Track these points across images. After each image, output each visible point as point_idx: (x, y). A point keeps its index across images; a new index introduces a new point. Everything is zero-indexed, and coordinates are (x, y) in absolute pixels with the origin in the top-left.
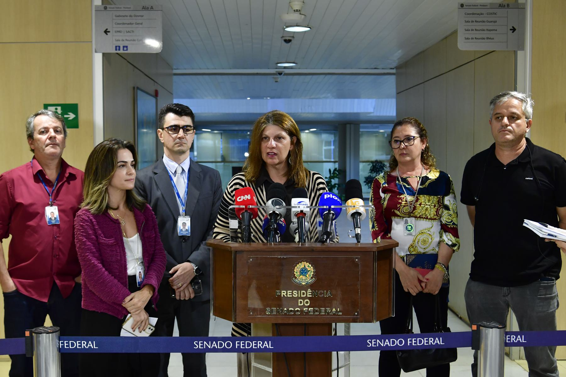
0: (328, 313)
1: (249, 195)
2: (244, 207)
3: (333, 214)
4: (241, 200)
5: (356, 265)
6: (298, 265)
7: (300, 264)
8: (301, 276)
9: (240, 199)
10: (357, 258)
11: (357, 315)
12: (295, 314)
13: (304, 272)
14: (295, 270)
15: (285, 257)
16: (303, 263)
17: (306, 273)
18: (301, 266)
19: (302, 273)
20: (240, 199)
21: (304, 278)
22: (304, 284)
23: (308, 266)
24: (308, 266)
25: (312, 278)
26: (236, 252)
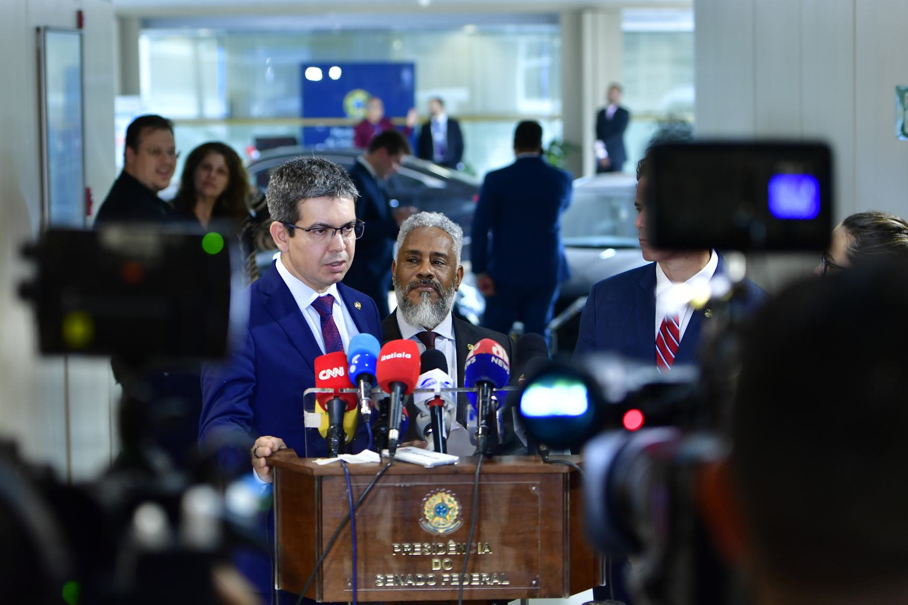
0: (485, 582)
1: (342, 368)
2: (331, 391)
3: (496, 401)
5: (534, 498)
6: (431, 500)
7: (434, 497)
8: (437, 519)
9: (325, 375)
10: (534, 485)
11: (535, 585)
12: (426, 586)
13: (441, 510)
14: (426, 509)
15: (408, 485)
16: (439, 494)
17: (444, 512)
18: (435, 500)
19: (439, 513)
20: (325, 375)
21: (441, 521)
22: (441, 531)
23: (450, 501)
24: (450, 501)
25: (456, 520)
26: (321, 478)
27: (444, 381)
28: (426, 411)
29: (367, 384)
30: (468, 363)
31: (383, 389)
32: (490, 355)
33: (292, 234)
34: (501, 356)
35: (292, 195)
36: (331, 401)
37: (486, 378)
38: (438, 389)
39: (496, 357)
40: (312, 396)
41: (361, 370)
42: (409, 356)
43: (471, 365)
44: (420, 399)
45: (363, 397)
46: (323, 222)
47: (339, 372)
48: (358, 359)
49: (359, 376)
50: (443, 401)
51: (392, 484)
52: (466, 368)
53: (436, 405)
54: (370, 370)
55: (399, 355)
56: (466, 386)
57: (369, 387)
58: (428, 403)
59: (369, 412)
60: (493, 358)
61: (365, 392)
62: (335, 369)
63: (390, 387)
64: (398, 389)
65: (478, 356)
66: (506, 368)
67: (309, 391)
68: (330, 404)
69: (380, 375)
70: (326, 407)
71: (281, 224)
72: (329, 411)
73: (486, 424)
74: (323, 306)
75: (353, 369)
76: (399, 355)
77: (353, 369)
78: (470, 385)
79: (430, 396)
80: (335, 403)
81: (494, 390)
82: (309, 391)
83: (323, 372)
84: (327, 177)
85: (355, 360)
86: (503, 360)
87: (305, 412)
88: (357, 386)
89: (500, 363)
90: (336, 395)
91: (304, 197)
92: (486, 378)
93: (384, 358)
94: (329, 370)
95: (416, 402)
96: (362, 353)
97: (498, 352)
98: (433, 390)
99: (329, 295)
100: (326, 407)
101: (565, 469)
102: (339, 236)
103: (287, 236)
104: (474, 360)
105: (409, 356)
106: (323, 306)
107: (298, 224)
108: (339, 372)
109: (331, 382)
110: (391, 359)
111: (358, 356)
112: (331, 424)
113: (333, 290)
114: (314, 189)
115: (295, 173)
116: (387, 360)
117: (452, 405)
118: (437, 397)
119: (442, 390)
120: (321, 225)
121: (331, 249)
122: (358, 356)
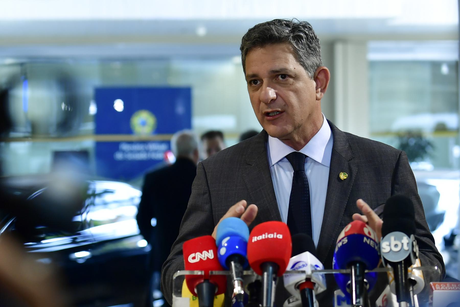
1: (211, 252)
4: (197, 260)
9: (194, 258)
20: (194, 258)
27: (314, 264)
28: (297, 294)
29: (238, 266)
30: (340, 244)
31: (255, 270)
32: (362, 235)
34: (372, 237)
36: (201, 284)
37: (358, 258)
38: (309, 271)
39: (368, 238)
40: (181, 278)
41: (231, 252)
43: (343, 246)
44: (291, 281)
45: (235, 278)
47: (209, 254)
48: (228, 242)
49: (230, 258)
50: (314, 284)
52: (337, 250)
53: (307, 286)
54: (242, 252)
55: (271, 236)
56: (335, 268)
58: (299, 286)
59: (242, 292)
60: (365, 239)
61: (236, 273)
62: (205, 252)
63: (261, 268)
64: (271, 268)
65: (349, 237)
67: (179, 273)
68: (200, 288)
69: (251, 257)
70: (196, 291)
72: (198, 295)
75: (223, 251)
76: (271, 236)
77: (223, 251)
78: (340, 265)
79: (301, 278)
80: (205, 286)
81: (366, 271)
82: (179, 273)
83: (193, 255)
85: (225, 243)
86: (374, 241)
87: (174, 296)
88: (229, 268)
90: (206, 278)
92: (358, 258)
93: (255, 239)
95: (286, 285)
96: (232, 235)
97: (369, 233)
98: (304, 272)
100: (196, 291)
104: (346, 241)
105: (280, 236)
108: (210, 254)
109: (201, 264)
110: (262, 240)
111: (228, 238)
117: (321, 287)
118: (308, 279)
119: (313, 272)
122: (228, 238)
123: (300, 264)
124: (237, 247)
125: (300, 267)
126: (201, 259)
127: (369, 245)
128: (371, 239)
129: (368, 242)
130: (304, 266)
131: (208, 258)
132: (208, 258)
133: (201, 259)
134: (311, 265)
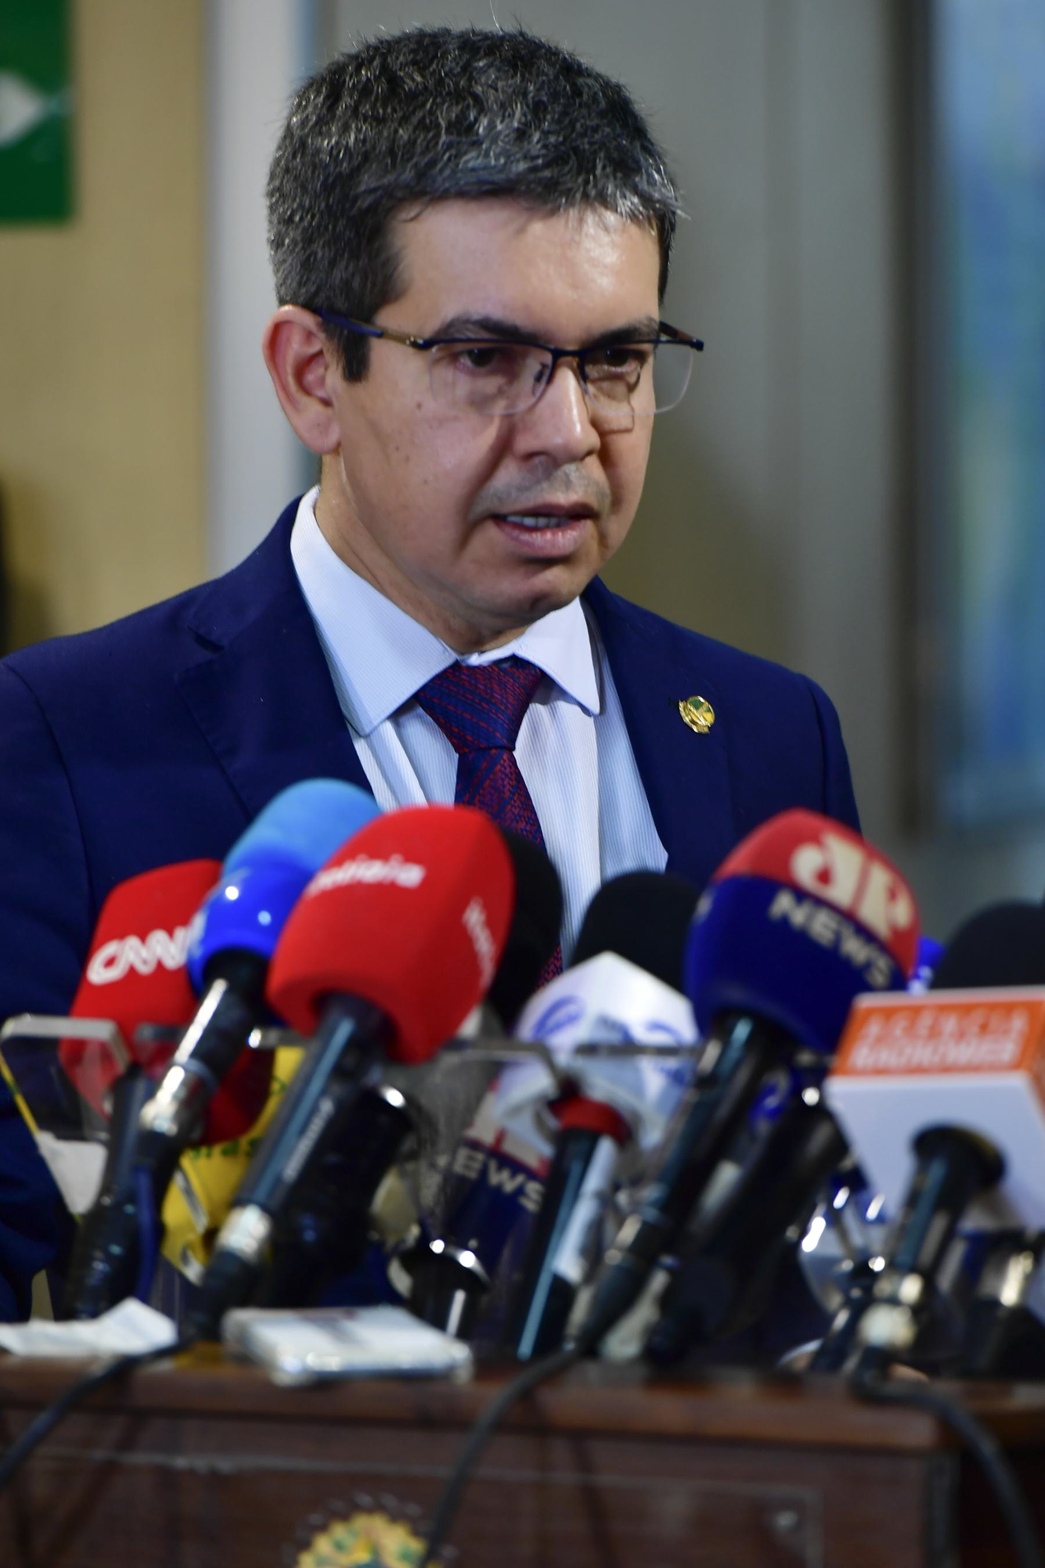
6: (323, 1545)
7: (339, 1531)
9: (110, 962)
15: (225, 1464)
16: (361, 1522)
20: (110, 962)
33: (356, 368)
34: (841, 892)
35: (367, 181)
37: (735, 993)
39: (801, 895)
41: (235, 936)
42: (411, 875)
46: (496, 312)
51: (158, 1459)
57: (236, 1014)
60: (783, 904)
62: (158, 937)
66: (855, 949)
71: (308, 320)
73: (665, 1206)
74: (478, 710)
84: (538, 109)
86: (849, 917)
89: (822, 926)
91: (427, 191)
93: (327, 880)
94: (133, 941)
97: (824, 876)
99: (515, 660)
101: (917, 1431)
102: (567, 381)
103: (331, 376)
105: (411, 875)
106: (478, 710)
107: (389, 318)
112: (106, 1188)
113: (560, 644)
114: (471, 159)
115: (394, 82)
116: (354, 891)
120: (486, 324)
121: (524, 443)
122: (243, 874)
123: (561, 1015)
124: (265, 918)
125: (559, 1026)
126: (132, 971)
127: (801, 938)
128: (820, 902)
129: (799, 916)
130: (573, 1019)
131: (160, 966)
132: (160, 966)
133: (132, 971)
134: (606, 1022)
